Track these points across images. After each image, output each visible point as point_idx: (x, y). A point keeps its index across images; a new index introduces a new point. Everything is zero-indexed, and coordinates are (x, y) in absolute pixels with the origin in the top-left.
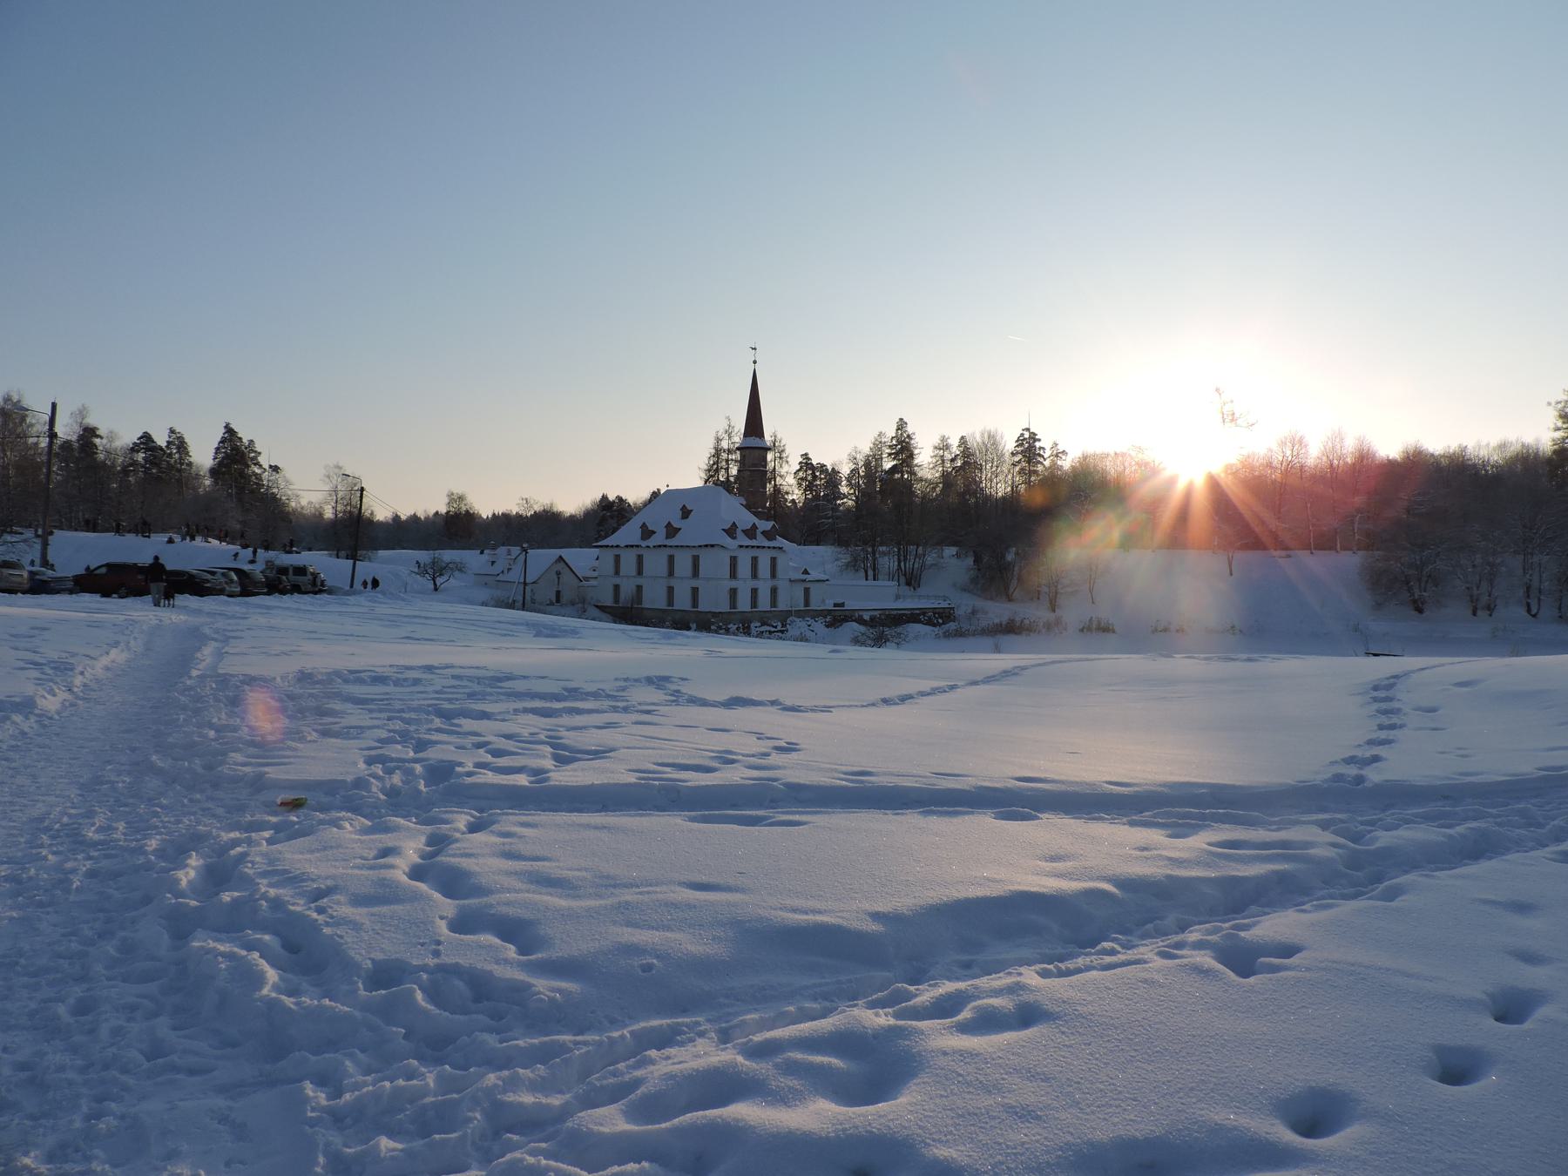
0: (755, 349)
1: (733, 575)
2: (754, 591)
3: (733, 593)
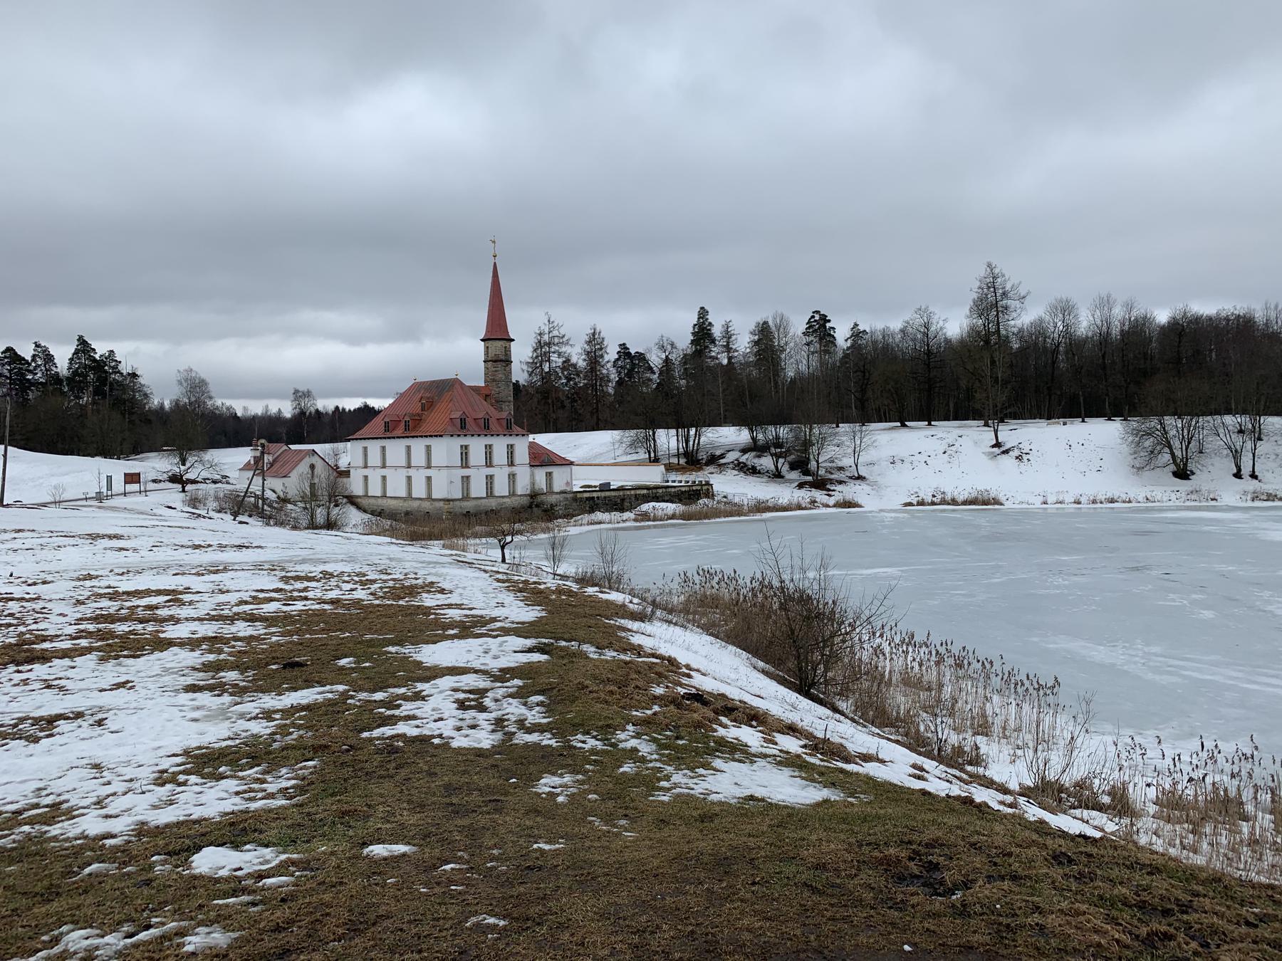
0: (494, 242)
1: (465, 463)
2: (490, 479)
3: (466, 479)
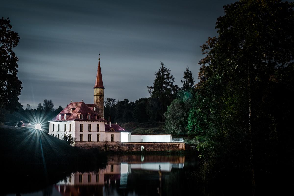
2: (90, 136)
3: (81, 136)
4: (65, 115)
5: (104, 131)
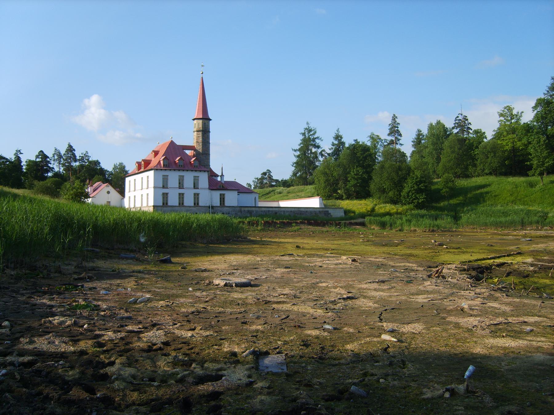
2: (181, 196)
3: (165, 195)
4: (143, 163)
5: (208, 187)
